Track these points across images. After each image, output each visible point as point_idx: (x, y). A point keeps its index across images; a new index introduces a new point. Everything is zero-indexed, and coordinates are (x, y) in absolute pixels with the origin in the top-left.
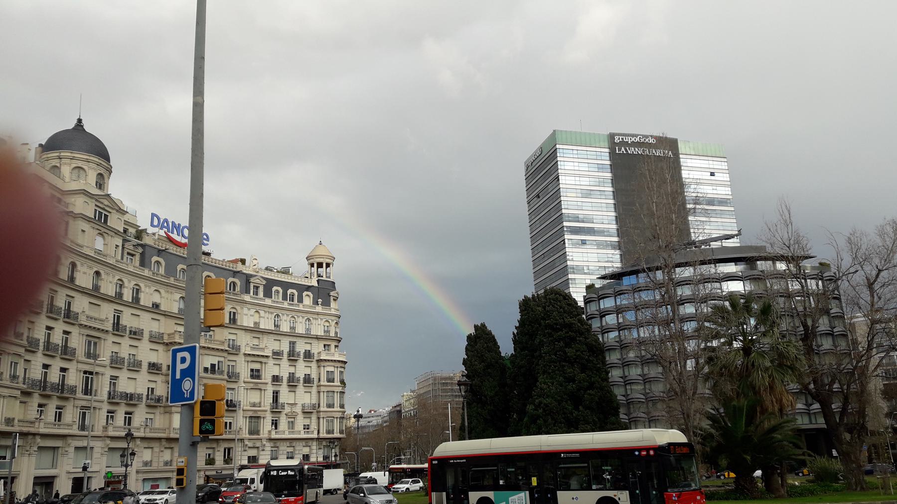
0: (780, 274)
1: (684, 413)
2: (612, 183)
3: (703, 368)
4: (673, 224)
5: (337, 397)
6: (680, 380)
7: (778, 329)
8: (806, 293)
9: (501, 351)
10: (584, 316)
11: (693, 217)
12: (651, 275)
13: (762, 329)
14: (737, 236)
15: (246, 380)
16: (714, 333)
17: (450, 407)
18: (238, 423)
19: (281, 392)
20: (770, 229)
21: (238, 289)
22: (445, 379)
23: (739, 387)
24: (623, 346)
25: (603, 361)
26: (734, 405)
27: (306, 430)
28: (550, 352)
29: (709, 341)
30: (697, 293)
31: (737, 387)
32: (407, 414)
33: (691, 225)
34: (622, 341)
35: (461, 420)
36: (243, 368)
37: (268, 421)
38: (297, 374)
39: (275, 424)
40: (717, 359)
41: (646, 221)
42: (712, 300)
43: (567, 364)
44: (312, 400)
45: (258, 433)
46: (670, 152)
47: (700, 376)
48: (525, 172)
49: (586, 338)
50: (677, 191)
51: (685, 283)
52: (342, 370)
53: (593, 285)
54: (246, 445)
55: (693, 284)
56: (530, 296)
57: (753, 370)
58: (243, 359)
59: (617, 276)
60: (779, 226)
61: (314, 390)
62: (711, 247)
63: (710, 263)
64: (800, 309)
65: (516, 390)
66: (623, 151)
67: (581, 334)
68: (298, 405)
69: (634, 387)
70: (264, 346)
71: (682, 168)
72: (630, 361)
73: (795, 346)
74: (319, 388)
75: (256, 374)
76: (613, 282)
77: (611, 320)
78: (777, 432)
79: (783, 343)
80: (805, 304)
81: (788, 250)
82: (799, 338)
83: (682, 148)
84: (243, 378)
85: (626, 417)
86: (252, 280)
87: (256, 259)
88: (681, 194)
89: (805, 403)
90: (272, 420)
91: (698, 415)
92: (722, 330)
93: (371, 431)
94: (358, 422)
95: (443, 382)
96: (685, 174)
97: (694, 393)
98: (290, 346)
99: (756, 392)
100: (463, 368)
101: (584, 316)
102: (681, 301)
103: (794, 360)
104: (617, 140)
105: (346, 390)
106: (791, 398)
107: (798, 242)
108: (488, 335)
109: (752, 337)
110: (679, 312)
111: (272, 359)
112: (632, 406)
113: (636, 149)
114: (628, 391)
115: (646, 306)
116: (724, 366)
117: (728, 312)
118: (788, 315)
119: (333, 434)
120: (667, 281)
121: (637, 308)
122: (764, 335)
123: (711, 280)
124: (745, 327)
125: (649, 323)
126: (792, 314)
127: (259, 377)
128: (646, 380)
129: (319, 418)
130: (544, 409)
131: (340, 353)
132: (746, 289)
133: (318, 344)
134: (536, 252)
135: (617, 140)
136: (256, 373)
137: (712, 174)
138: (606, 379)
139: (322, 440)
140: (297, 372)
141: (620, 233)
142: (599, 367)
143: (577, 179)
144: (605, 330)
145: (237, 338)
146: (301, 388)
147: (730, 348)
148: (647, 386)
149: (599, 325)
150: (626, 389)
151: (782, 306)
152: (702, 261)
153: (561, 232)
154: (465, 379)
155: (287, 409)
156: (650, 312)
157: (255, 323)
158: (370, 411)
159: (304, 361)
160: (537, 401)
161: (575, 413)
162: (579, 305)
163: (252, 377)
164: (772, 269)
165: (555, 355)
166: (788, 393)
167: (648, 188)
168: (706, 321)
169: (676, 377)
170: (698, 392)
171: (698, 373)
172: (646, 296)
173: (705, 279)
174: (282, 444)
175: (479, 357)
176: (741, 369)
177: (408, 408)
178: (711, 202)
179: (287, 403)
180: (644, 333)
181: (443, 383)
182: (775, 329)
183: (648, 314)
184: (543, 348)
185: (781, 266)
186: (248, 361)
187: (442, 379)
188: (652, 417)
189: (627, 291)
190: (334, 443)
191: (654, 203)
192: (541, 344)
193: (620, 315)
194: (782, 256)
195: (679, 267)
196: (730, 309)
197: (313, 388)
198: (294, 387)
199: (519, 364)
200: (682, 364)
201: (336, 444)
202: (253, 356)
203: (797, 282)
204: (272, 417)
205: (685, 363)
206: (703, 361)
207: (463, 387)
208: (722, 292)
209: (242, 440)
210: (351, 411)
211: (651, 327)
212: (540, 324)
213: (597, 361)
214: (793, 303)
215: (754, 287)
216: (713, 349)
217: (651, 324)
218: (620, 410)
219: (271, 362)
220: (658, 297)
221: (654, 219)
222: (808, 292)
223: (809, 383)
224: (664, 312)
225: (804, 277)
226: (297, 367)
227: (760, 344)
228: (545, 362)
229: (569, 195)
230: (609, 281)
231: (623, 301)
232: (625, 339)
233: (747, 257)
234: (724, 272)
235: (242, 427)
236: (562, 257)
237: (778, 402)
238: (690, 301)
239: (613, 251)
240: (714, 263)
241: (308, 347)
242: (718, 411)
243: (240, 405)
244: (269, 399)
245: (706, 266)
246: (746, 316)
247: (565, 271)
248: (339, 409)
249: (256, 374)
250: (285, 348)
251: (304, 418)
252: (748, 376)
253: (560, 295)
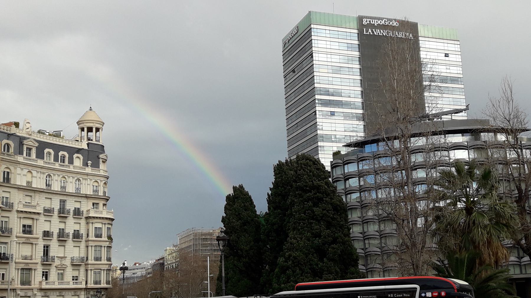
0: (500, 144)
1: (413, 265)
2: (360, 61)
3: (431, 225)
4: (410, 99)
5: (104, 251)
6: (411, 236)
7: (496, 192)
8: (521, 161)
9: (256, 210)
10: (330, 179)
11: (428, 93)
12: (389, 144)
13: (483, 192)
14: (465, 111)
16: (441, 195)
17: (209, 260)
18: (10, 274)
19: (51, 246)
20: (493, 105)
21: (12, 150)
22: (206, 234)
23: (461, 242)
24: (363, 206)
25: (346, 219)
26: (457, 258)
27: (75, 281)
28: (300, 210)
29: (437, 202)
30: (428, 160)
31: (460, 242)
32: (170, 266)
33: (426, 100)
34: (362, 201)
35: (219, 271)
36: (16, 224)
37: (39, 273)
38: (66, 230)
39: (46, 275)
40: (443, 217)
41: (387, 95)
42: (441, 166)
43: (315, 221)
44: (80, 254)
45: (29, 283)
46: (411, 34)
47: (428, 232)
48: (283, 48)
49: (331, 199)
50: (415, 70)
51: (418, 151)
52: (110, 226)
53: (339, 152)
54: (19, 295)
55: (425, 152)
56: (284, 161)
57: (474, 228)
58: (16, 216)
59: (360, 145)
60: (501, 103)
61: (83, 245)
62: (442, 120)
63: (441, 134)
64: (516, 175)
65: (268, 244)
66: (370, 33)
67: (328, 195)
68: (67, 258)
69: (372, 242)
71: (421, 49)
72: (370, 219)
73: (510, 207)
74: (87, 243)
75: (27, 230)
76: (356, 149)
77: (353, 182)
78: (492, 281)
79: (500, 204)
80: (520, 170)
81: (508, 124)
82: (514, 200)
83: (421, 31)
84: (15, 233)
85: (364, 268)
86: (25, 142)
87: (29, 123)
88: (419, 73)
89: (517, 256)
90: (43, 272)
91: (425, 266)
92: (448, 192)
93: (136, 281)
94: (124, 274)
95: (204, 238)
96: (423, 55)
97: (423, 247)
98: (60, 204)
99: (476, 247)
100: (222, 225)
101: (330, 179)
102: (414, 166)
103: (510, 219)
104: (364, 22)
105: (113, 245)
106: (505, 251)
107: (517, 117)
108: (245, 195)
109: (474, 199)
110: (412, 177)
111: (43, 216)
112: (369, 258)
113: (382, 31)
114: (366, 245)
115: (384, 171)
116: (449, 224)
117: (454, 177)
118: (505, 180)
119: (100, 284)
120: (403, 149)
121: (376, 173)
122: (484, 197)
123: (440, 149)
124: (468, 190)
125: (386, 186)
126: (509, 179)
127: (30, 232)
128: (382, 236)
129: (87, 270)
130: (293, 261)
131: (108, 211)
132: (471, 157)
133: (87, 202)
134: (290, 122)
136: (28, 229)
137: (447, 55)
138: (348, 235)
139: (90, 290)
140: (66, 228)
141: (365, 106)
142: (342, 224)
143: (329, 56)
144: (348, 192)
145: (10, 196)
146: (70, 243)
147: (455, 208)
148: (383, 241)
149: (343, 187)
150: (365, 244)
151: (500, 172)
152: (434, 132)
153: (313, 104)
154: (223, 234)
155: (57, 262)
156: (387, 176)
157: (28, 182)
158: (135, 264)
159: (74, 218)
160: (287, 254)
161: (320, 264)
162: (326, 169)
163: (24, 232)
164: (494, 140)
165: (305, 213)
166: (503, 247)
167: (390, 66)
168: (435, 185)
169: (408, 233)
170: (427, 246)
171: (427, 229)
172: (384, 162)
173: (435, 148)
174: (52, 293)
175: (237, 215)
176: (464, 227)
177: (170, 261)
178: (444, 80)
179: (57, 257)
180: (382, 194)
181: (204, 238)
182: (494, 192)
183: (385, 178)
184: (294, 207)
185: (501, 137)
186: (20, 218)
187: (202, 235)
188: (386, 267)
189: (369, 158)
190: (101, 293)
191: (395, 80)
192: (292, 204)
193: (361, 179)
194: (502, 128)
195: (414, 137)
196: (456, 174)
197: (82, 243)
198: (64, 242)
199: (272, 221)
200: (414, 221)
201: (102, 293)
202: (25, 213)
203: (514, 152)
204: (43, 269)
205: (416, 221)
206: (431, 219)
207: (221, 242)
208: (450, 159)
209: (14, 290)
210: (117, 264)
211: (388, 189)
212: (291, 186)
213: (340, 219)
214: (510, 170)
215: (478, 155)
216: (440, 209)
217: (388, 186)
218: (359, 262)
219: (42, 218)
220: (395, 163)
221: (394, 94)
222: (523, 160)
223: (521, 239)
224: (399, 176)
225: (520, 147)
226: (66, 223)
227: (480, 205)
228: (295, 219)
229: (321, 70)
230: (353, 148)
231: (365, 166)
232: (365, 199)
233: (472, 129)
234: (452, 142)
235: (14, 278)
236: (313, 126)
237: (495, 255)
238: (422, 166)
239: (357, 122)
240: (444, 134)
241: (77, 205)
242: (443, 263)
243: (12, 258)
244: (40, 253)
245: (437, 136)
246: (470, 180)
247: (315, 139)
248: (106, 262)
249: (27, 230)
250: (56, 205)
251: (73, 270)
252: (470, 232)
253: (311, 160)
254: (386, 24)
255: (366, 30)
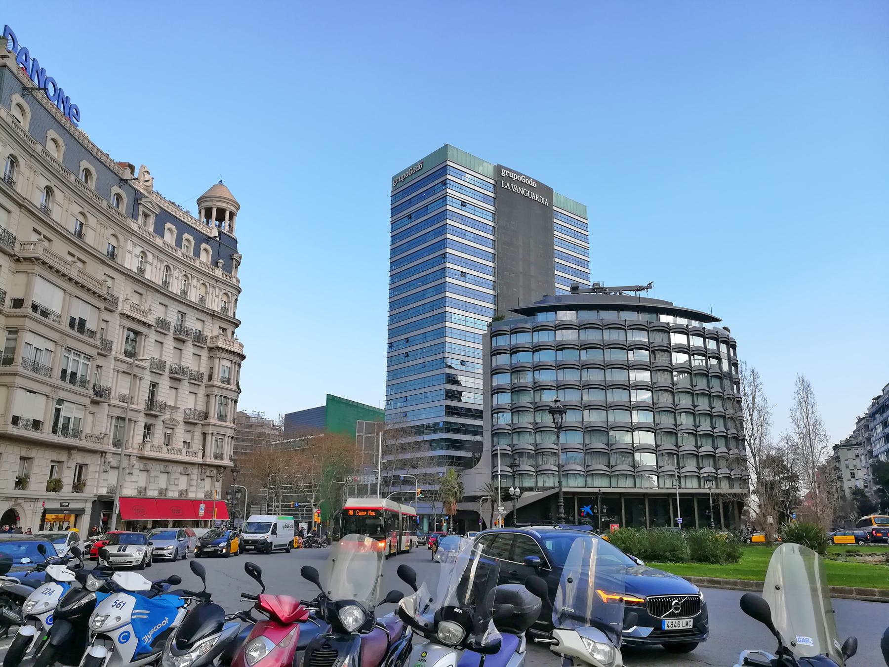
15: (118, 356)
19: (160, 385)
58: (118, 323)
61: (202, 392)
70: (147, 309)
74: (209, 389)
111: (154, 332)
129: (204, 435)
133: (213, 324)
146: (185, 387)
198: (177, 382)
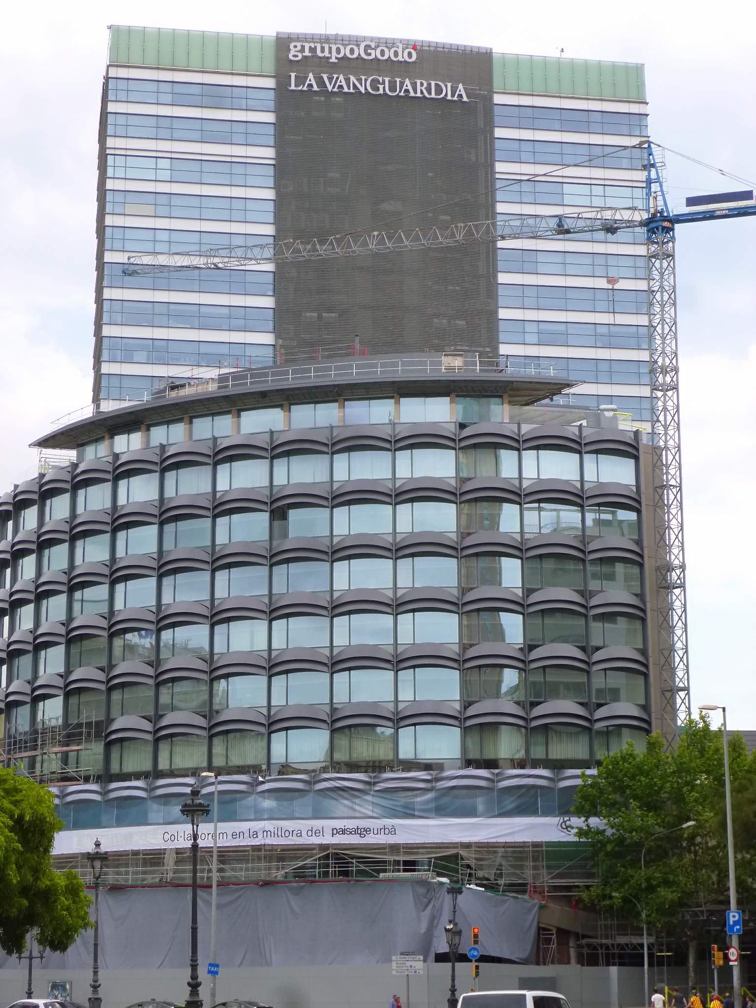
66: (310, 85)
113: (353, 79)
135: (294, 54)
254: (373, 56)
255: (452, 86)
